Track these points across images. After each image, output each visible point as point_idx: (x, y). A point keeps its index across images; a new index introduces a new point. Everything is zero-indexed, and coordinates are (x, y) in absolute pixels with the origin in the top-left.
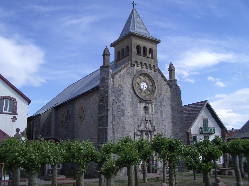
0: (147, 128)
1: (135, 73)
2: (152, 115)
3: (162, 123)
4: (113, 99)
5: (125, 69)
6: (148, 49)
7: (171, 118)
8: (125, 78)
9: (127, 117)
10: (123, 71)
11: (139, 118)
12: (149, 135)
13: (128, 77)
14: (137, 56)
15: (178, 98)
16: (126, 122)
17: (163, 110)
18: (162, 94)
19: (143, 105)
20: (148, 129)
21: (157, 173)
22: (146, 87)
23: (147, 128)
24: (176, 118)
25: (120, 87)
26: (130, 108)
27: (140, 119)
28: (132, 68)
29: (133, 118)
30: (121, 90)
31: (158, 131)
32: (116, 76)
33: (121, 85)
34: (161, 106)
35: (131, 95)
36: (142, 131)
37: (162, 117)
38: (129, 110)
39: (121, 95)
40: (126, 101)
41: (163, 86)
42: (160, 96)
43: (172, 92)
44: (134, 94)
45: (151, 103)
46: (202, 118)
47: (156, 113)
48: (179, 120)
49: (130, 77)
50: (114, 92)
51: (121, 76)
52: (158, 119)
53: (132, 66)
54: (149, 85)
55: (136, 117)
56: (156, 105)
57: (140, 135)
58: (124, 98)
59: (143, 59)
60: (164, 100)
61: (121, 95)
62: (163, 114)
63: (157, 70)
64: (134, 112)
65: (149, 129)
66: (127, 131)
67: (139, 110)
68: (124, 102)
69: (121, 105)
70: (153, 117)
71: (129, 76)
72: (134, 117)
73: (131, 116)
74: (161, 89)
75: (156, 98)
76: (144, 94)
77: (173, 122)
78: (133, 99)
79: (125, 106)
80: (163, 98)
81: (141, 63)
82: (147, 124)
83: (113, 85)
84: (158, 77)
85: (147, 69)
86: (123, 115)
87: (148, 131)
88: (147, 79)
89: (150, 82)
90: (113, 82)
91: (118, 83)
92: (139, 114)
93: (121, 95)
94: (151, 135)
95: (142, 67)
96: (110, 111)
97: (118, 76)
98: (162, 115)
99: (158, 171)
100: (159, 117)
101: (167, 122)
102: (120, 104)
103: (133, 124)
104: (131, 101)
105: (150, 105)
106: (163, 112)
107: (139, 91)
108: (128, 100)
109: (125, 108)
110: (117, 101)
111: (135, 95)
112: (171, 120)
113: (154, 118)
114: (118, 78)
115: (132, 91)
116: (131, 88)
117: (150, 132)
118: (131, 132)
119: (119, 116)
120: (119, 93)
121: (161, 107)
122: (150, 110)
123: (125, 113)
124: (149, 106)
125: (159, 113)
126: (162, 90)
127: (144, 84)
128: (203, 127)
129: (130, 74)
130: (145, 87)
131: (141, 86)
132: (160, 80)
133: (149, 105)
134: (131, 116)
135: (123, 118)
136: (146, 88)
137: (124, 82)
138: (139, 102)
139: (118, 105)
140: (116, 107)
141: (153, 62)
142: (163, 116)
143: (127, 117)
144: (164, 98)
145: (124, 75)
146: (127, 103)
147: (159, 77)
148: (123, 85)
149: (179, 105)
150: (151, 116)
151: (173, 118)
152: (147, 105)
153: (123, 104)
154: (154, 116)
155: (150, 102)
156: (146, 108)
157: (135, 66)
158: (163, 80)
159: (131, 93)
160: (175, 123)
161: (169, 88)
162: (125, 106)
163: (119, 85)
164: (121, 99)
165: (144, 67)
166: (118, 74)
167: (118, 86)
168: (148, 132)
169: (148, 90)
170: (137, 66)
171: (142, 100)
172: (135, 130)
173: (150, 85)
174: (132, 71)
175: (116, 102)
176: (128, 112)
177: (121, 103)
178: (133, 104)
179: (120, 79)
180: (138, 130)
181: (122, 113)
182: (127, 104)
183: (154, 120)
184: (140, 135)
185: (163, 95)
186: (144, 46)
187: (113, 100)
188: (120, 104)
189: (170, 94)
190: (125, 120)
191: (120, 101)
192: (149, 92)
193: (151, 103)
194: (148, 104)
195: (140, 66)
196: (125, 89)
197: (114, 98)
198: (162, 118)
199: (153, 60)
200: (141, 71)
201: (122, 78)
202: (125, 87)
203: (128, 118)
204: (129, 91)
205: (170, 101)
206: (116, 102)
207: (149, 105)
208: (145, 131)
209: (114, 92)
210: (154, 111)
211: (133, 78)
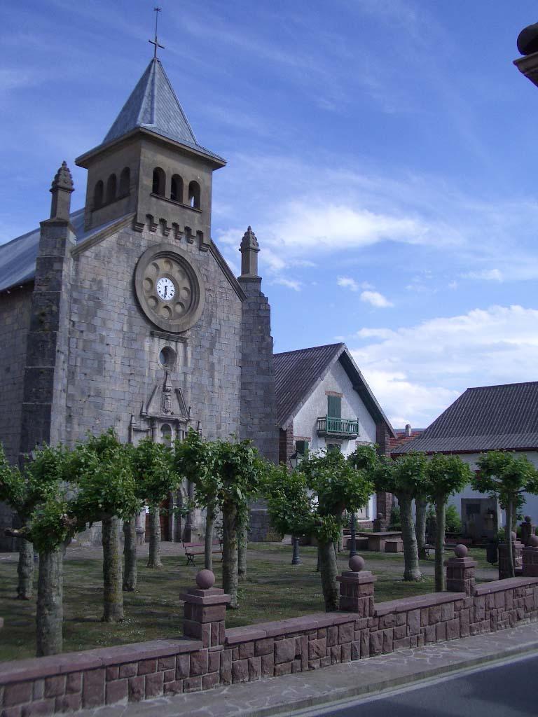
0: (167, 412)
1: (143, 249)
2: (185, 374)
3: (211, 399)
4: (74, 322)
5: (115, 236)
6: (186, 183)
7: (238, 385)
8: (114, 260)
10: (107, 239)
11: (146, 380)
12: (173, 432)
13: (121, 259)
14: (154, 199)
15: (261, 331)
16: (107, 392)
17: (215, 361)
19: (159, 344)
20: (169, 414)
21: (190, 542)
22: (173, 293)
23: (167, 412)
24: (253, 387)
25: (95, 288)
26: (121, 352)
27: (148, 384)
28: (137, 233)
29: (129, 381)
30: (97, 295)
31: (199, 422)
32: (87, 253)
33: (100, 281)
34: (211, 350)
35: (126, 313)
36: (152, 421)
38: (117, 357)
39: (96, 312)
40: (110, 329)
42: (210, 323)
43: (244, 312)
44: (136, 309)
45: (184, 341)
46: (327, 392)
47: (196, 369)
48: (261, 393)
49: (128, 258)
50: (76, 301)
51: (102, 254)
52: (201, 386)
53: (134, 230)
54: (181, 286)
55: (136, 378)
56: (196, 346)
58: (104, 321)
59: (170, 210)
60: (222, 335)
61: (98, 311)
62: (216, 373)
63: (207, 245)
64: (132, 364)
65: (172, 414)
66: (109, 416)
67: (147, 357)
68: (104, 333)
69: (94, 341)
70: (185, 381)
71: (123, 257)
72: (131, 378)
73: (123, 374)
74: (215, 304)
75: (200, 326)
76: (165, 313)
77: (243, 398)
78: (130, 325)
79: (107, 345)
80: (218, 328)
81: (163, 221)
82: (167, 399)
83: (75, 281)
84: (208, 266)
85: (180, 239)
86: (100, 370)
87: (169, 420)
88: (175, 270)
89: (184, 278)
90: (77, 272)
91: (91, 276)
92: (147, 370)
93: (98, 311)
94: (178, 431)
95: (164, 235)
96: (62, 357)
97: (94, 255)
98: (212, 376)
99: (193, 537)
100: (205, 381)
101: (227, 397)
102: (92, 337)
103: (127, 397)
104: (125, 329)
105: (180, 345)
106: (217, 367)
107: (152, 302)
108: (118, 326)
109: (107, 348)
110: (84, 327)
111: (138, 315)
112: (236, 392)
113: (189, 385)
114: (92, 260)
115: (130, 301)
116: (128, 294)
117: (176, 423)
118: (121, 422)
119: (88, 371)
120: (91, 303)
121: (212, 354)
122: (180, 360)
123: (107, 366)
124: (177, 350)
125: (204, 371)
127: (165, 284)
128: (326, 418)
129: (128, 252)
130: (169, 292)
131: (158, 290)
132: (213, 276)
133: (176, 345)
134: (123, 374)
135: (98, 378)
136: (171, 297)
137: (110, 273)
138: (148, 334)
139: (85, 341)
140: (81, 345)
141: (196, 222)
142: (216, 381)
143: (111, 377)
144: (223, 328)
145: (110, 252)
146: (112, 335)
147: (213, 266)
148: (105, 279)
149: (264, 352)
150: (182, 378)
151: (244, 386)
152: (173, 346)
153: (102, 339)
154: (189, 378)
155: (179, 337)
156: (167, 354)
157: (145, 228)
158: (223, 278)
159: (128, 306)
160: (249, 401)
161: (239, 301)
162: (107, 345)
163: (94, 280)
164: (97, 322)
165: (172, 233)
166: (93, 248)
167: (90, 285)
168: (170, 424)
169: (177, 300)
170: (151, 230)
171: (156, 330)
172: (132, 416)
173: (185, 289)
174: (134, 244)
175: (82, 332)
176: (115, 363)
177: (96, 336)
178: (130, 340)
179: (96, 263)
180: (142, 416)
181: (96, 365)
182: (114, 337)
183: (190, 391)
184: (147, 431)
185: (220, 320)
187: (72, 323)
188: (92, 337)
189: (239, 319)
190: (105, 386)
191: (92, 328)
192: (179, 309)
193: (184, 341)
194: (174, 343)
195: (159, 229)
196: (109, 295)
197: (75, 318)
198: (213, 385)
199: (198, 215)
200: (160, 245)
201: (104, 260)
202: (111, 289)
203: (113, 380)
204: (121, 300)
205: (237, 338)
206: (82, 332)
207: (176, 345)
208: (160, 420)
209: (76, 301)
210: (189, 364)
211: (137, 264)
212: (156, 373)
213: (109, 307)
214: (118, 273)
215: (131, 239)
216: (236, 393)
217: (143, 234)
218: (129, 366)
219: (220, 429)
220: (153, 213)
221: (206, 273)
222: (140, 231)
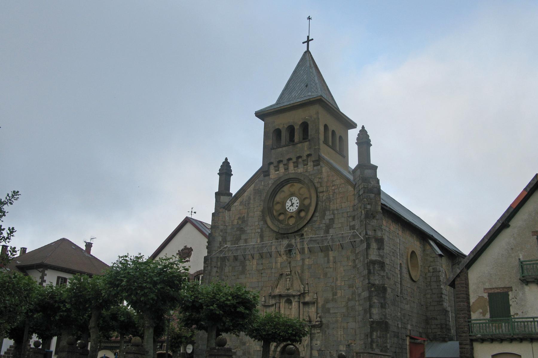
0: (288, 290)
5: (253, 186)
9: (249, 274)
10: (248, 190)
18: (331, 209)
25: (240, 222)
32: (236, 204)
37: (328, 259)
41: (334, 190)
53: (265, 176)
57: (272, 305)
60: (336, 221)
72: (263, 272)
73: (258, 271)
80: (332, 217)
87: (288, 296)
91: (237, 217)
92: (274, 264)
97: (239, 203)
101: (342, 269)
113: (306, 267)
126: (330, 202)
143: (249, 274)
144: (336, 216)
163: (239, 218)
179: (241, 207)
181: (241, 269)
184: (272, 305)
186: (288, 125)
196: (249, 223)
204: (257, 223)
208: (280, 296)
212: (281, 264)
213: (248, 231)
214: (254, 208)
215: (263, 183)
216: (350, 264)
217: (271, 176)
218: (262, 264)
219: (336, 296)
220: (272, 160)
221: (320, 180)
222: (269, 175)
